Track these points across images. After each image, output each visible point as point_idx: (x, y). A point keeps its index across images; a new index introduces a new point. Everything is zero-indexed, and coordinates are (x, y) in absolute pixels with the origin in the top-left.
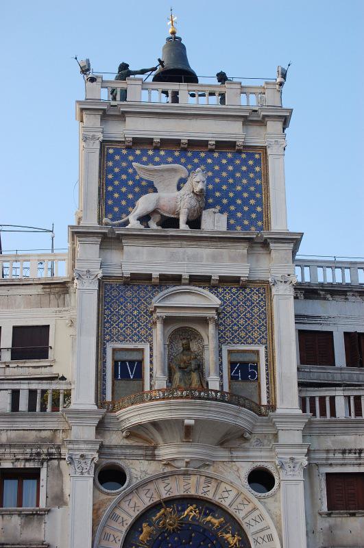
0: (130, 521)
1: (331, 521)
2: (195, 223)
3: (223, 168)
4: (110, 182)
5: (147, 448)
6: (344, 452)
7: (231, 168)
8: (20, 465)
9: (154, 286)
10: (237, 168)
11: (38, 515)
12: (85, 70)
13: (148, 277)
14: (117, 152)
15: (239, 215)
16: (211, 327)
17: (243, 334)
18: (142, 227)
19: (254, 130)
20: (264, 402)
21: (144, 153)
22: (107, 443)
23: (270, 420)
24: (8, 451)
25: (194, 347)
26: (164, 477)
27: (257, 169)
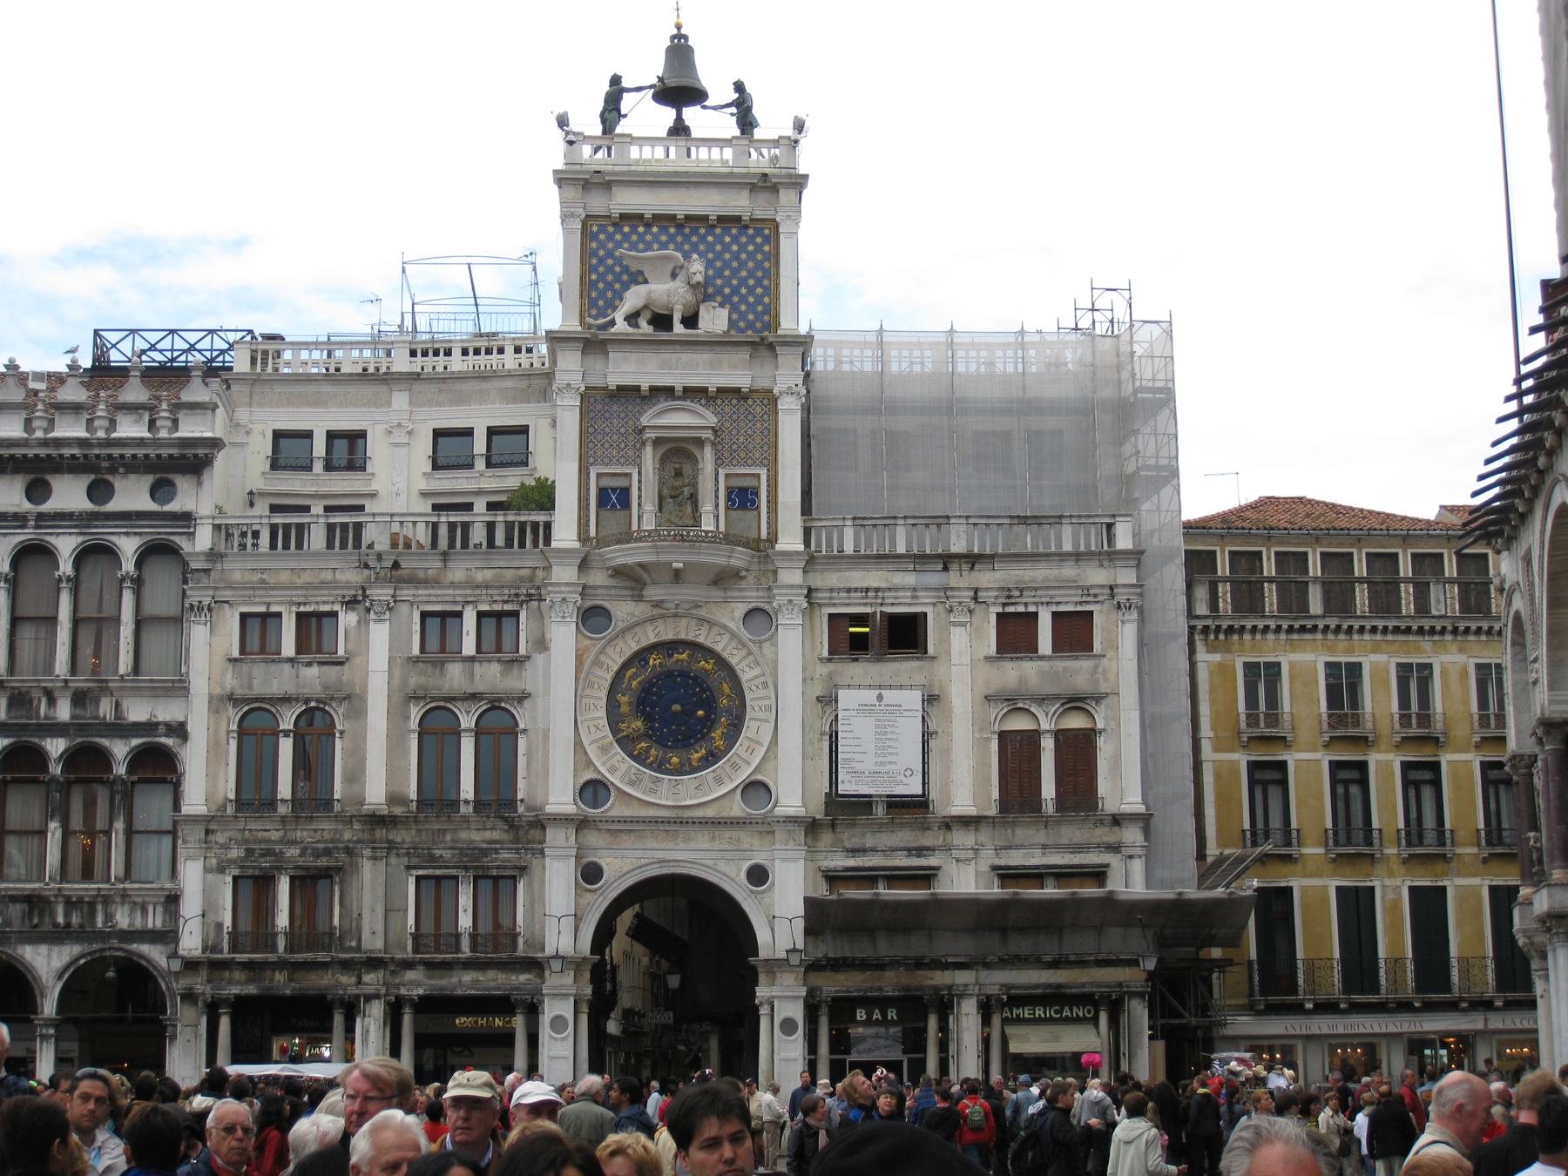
0: (616, 668)
1: (832, 666)
2: (691, 321)
3: (726, 247)
4: (594, 269)
5: (633, 589)
6: (849, 590)
7: (735, 248)
8: (497, 607)
9: (643, 398)
10: (743, 248)
11: (519, 661)
12: (562, 122)
13: (638, 388)
14: (602, 229)
15: (743, 308)
16: (708, 453)
17: (743, 455)
18: (630, 330)
19: (763, 198)
20: (764, 534)
21: (634, 229)
22: (591, 583)
23: (767, 556)
25: (687, 469)
26: (653, 619)
27: (766, 248)
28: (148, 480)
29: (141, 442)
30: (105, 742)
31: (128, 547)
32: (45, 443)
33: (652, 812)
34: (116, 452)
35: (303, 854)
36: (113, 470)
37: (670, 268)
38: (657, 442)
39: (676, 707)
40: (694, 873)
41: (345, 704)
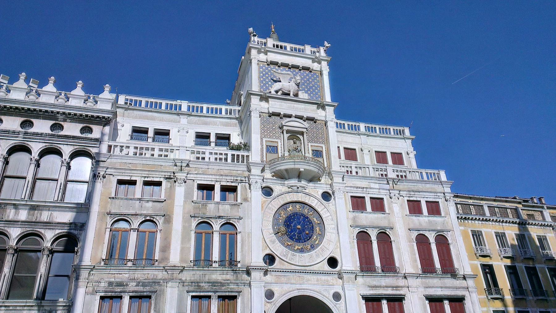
2: (296, 95)
6: (357, 188)
10: (310, 78)
19: (316, 64)
24: (224, 177)
28: (81, 126)
29: (79, 108)
30: (42, 231)
31: (67, 150)
32: (34, 103)
33: (293, 267)
34: (67, 111)
35: (137, 285)
36: (65, 120)
37: (289, 77)
38: (288, 132)
39: (299, 227)
40: (311, 295)
41: (163, 218)
